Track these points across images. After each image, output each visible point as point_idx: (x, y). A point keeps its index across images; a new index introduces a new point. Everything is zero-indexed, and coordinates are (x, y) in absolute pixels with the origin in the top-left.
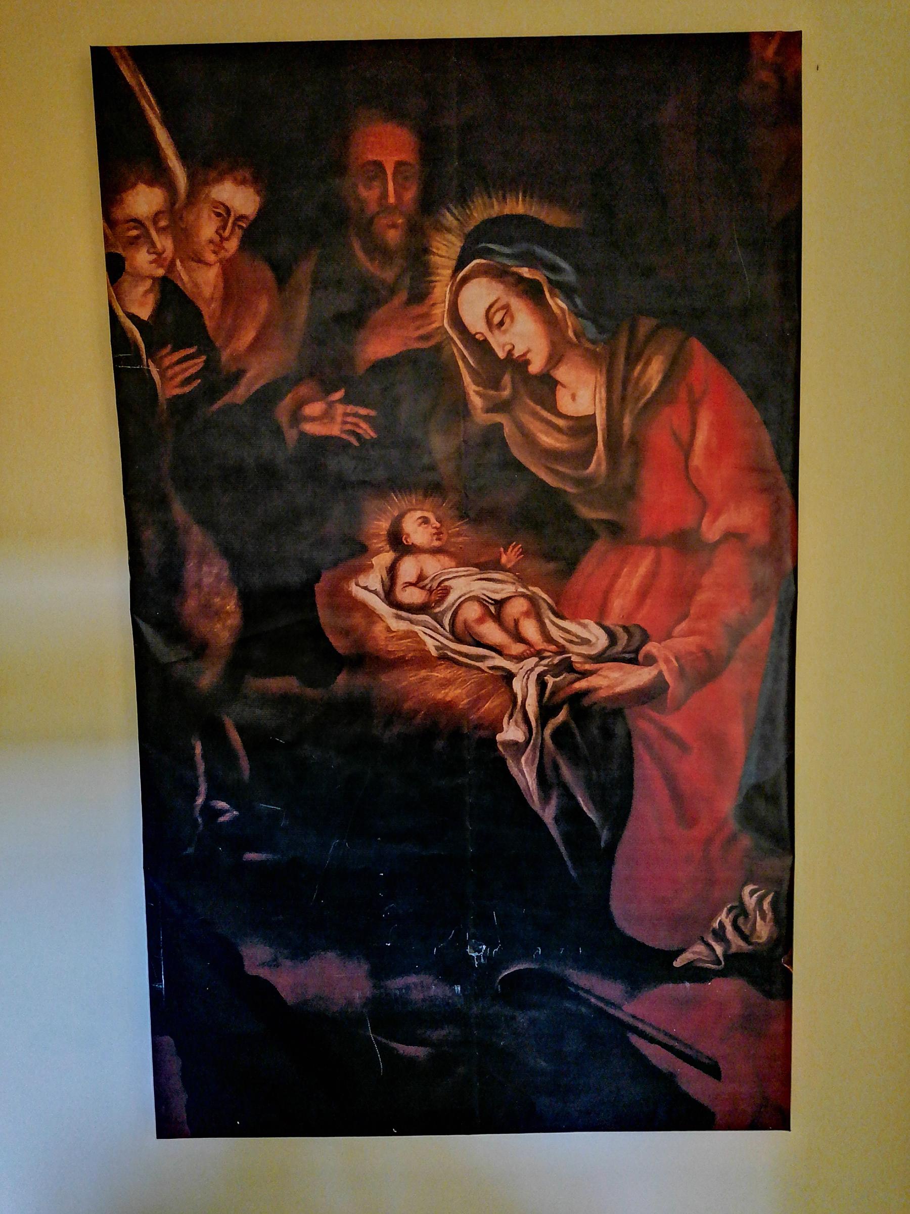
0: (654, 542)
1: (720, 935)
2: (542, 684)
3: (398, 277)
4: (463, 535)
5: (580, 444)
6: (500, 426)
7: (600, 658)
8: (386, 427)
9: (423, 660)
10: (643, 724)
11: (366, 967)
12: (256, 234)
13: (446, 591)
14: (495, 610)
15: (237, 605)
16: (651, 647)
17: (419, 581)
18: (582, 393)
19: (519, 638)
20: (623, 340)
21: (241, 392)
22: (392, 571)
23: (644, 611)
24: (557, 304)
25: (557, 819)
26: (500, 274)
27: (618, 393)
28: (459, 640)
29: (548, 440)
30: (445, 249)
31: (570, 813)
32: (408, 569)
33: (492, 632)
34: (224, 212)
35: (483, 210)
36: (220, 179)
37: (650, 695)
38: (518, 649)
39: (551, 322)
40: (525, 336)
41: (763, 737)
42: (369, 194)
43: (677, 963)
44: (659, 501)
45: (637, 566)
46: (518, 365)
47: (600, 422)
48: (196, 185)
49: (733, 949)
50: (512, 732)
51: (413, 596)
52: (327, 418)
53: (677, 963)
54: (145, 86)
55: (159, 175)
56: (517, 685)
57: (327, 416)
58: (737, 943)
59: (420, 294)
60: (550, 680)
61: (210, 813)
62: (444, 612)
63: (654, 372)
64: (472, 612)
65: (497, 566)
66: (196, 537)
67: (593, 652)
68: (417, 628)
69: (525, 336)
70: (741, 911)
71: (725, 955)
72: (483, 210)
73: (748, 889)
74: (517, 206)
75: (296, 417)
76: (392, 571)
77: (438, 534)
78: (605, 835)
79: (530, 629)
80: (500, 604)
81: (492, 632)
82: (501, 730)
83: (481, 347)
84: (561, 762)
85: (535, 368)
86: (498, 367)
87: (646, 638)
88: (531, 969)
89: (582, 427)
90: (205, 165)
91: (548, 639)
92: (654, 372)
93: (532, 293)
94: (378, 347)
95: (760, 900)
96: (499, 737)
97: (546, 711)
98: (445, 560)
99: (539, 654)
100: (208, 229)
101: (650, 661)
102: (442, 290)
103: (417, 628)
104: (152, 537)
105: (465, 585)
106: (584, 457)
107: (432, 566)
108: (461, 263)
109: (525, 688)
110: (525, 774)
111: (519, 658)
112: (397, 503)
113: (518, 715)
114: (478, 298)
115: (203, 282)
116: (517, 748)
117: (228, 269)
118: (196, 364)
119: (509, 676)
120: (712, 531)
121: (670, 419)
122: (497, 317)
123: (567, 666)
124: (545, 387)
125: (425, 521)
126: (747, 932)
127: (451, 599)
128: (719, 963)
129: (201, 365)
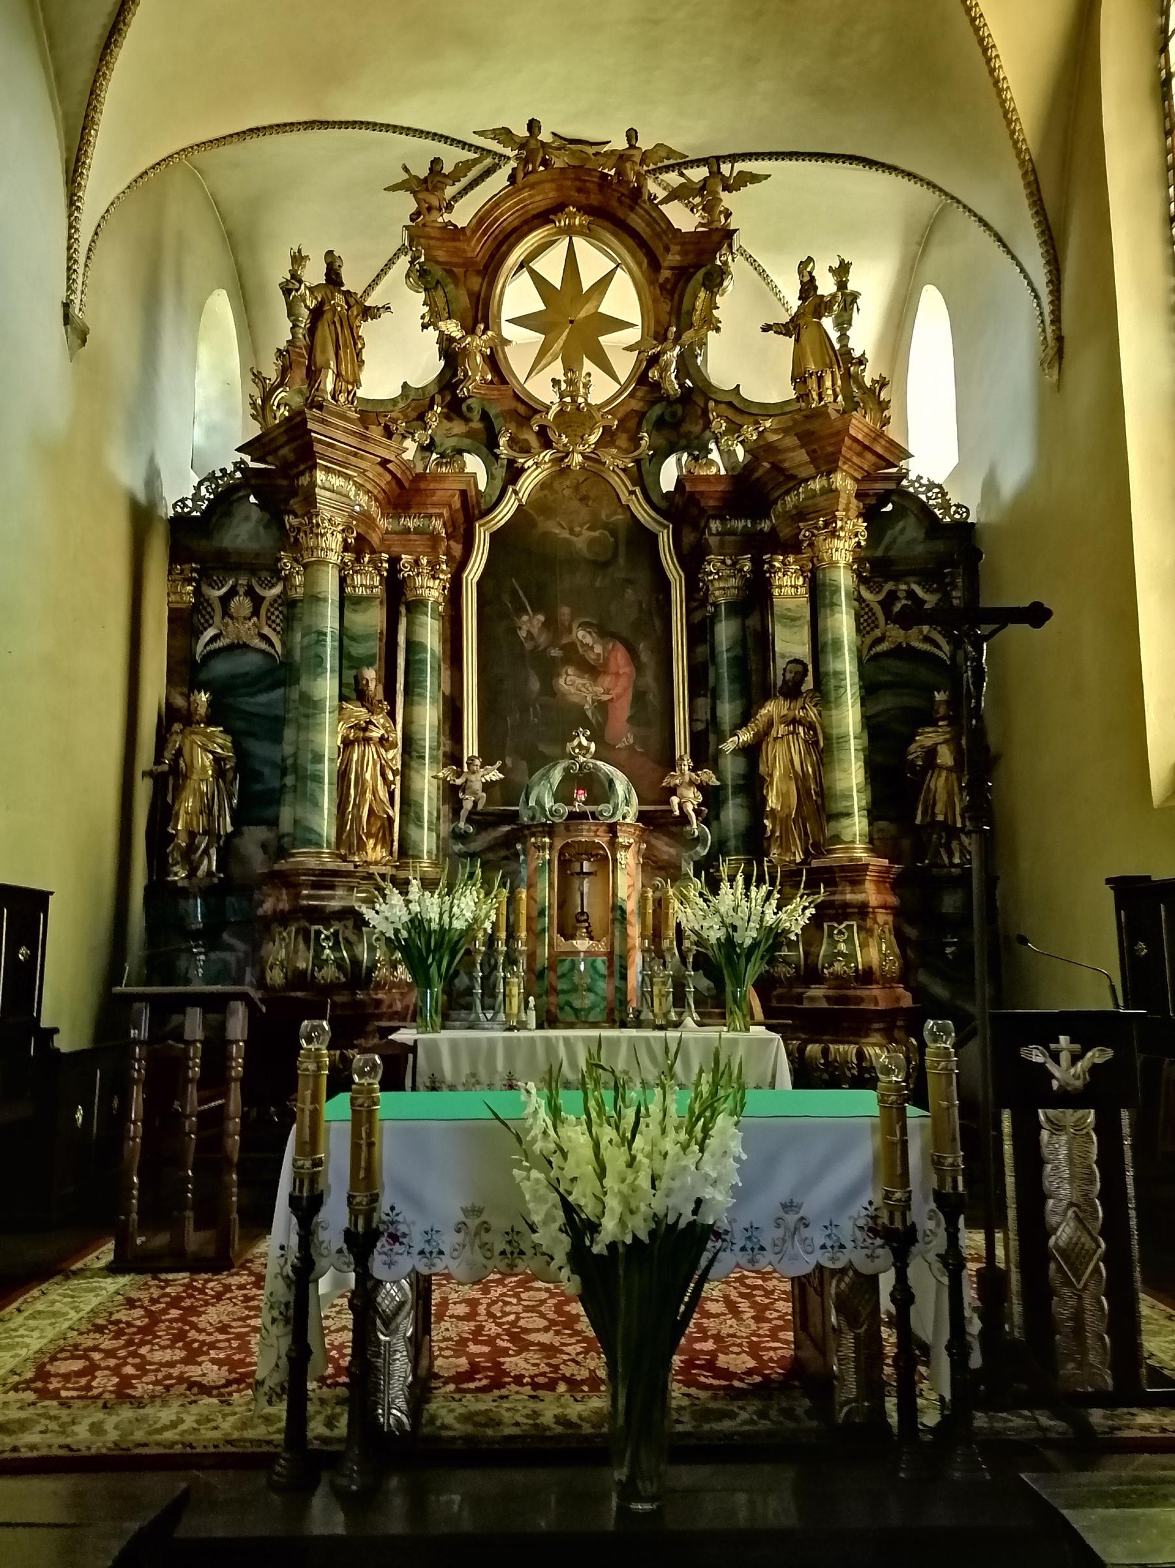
12: (544, 624)
14: (584, 685)
18: (598, 649)
27: (604, 649)
30: (575, 626)
31: (597, 721)
32: (569, 678)
40: (588, 640)
44: (613, 668)
50: (587, 707)
52: (555, 653)
55: (528, 614)
59: (571, 632)
69: (588, 640)
86: (583, 645)
89: (599, 654)
90: (536, 611)
93: (590, 633)
94: (564, 641)
97: (593, 702)
100: (535, 622)
105: (579, 681)
109: (589, 699)
110: (589, 714)
114: (581, 634)
115: (535, 631)
120: (621, 672)
121: (614, 653)
122: (584, 637)
124: (592, 648)
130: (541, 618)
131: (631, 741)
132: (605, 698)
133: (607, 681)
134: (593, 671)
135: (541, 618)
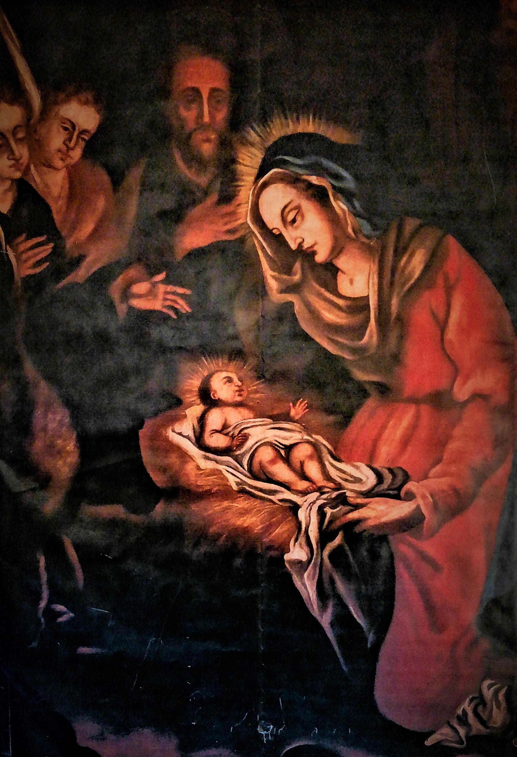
0: (414, 400)
1: (463, 720)
2: (321, 513)
3: (211, 182)
4: (259, 392)
5: (356, 320)
6: (291, 305)
7: (369, 494)
8: (199, 303)
9: (226, 493)
10: (403, 547)
11: (175, 741)
12: (96, 146)
13: (246, 438)
14: (285, 453)
15: (75, 446)
16: (410, 486)
17: (224, 429)
18: (358, 279)
19: (304, 477)
20: (392, 236)
21: (81, 274)
22: (202, 420)
23: (406, 457)
24: (340, 206)
25: (332, 624)
26: (294, 181)
28: (255, 477)
29: (330, 316)
30: (249, 160)
31: (343, 619)
32: (215, 419)
33: (281, 471)
34: (70, 127)
35: (280, 128)
36: (67, 100)
37: (409, 525)
38: (303, 485)
39: (334, 221)
40: (312, 231)
41: (501, 560)
42: (188, 115)
43: (428, 743)
44: (420, 369)
45: (400, 420)
46: (307, 255)
47: (373, 302)
48: (48, 105)
49: (474, 732)
50: (297, 553)
51: (219, 441)
52: (152, 295)
53: (428, 743)
54: (8, 24)
56: (302, 514)
57: (151, 293)
58: (477, 727)
59: (227, 197)
60: (329, 511)
61: (51, 615)
62: (244, 454)
63: (416, 263)
64: (266, 455)
65: (287, 417)
66: (44, 391)
67: (364, 488)
68: (221, 467)
69: (312, 231)
70: (480, 701)
71: (467, 737)
72: (280, 128)
73: (486, 683)
74: (308, 126)
75: (126, 294)
76: (202, 420)
77: (240, 391)
78: (371, 637)
79: (313, 469)
80: (289, 448)
81: (281, 471)
82: (288, 551)
83: (277, 240)
84: (337, 578)
85: (321, 257)
86: (291, 256)
87: (407, 478)
88: (309, 746)
89: (359, 306)
90: (56, 89)
91: (328, 477)
92: (416, 263)
93: (319, 196)
94: (194, 238)
95: (496, 693)
96: (287, 557)
98: (245, 412)
99: (320, 490)
100: (57, 140)
101: (410, 497)
102: (246, 193)
103: (221, 467)
104: (8, 390)
105: (261, 433)
106: (359, 331)
107: (235, 417)
108: (262, 171)
109: (308, 517)
110: (307, 587)
111: (304, 493)
112: (207, 365)
113: (302, 539)
114: (276, 199)
115: (53, 184)
116: (301, 566)
117: (73, 175)
118: (45, 250)
119: (295, 508)
120: (462, 392)
121: (429, 301)
122: (291, 217)
123: (342, 500)
125: (230, 380)
126: (485, 718)
127: (249, 443)
128: (462, 743)
129: (50, 251)
130: (85, 116)
131: (498, 717)
132: (382, 512)
133: (390, 430)
134: (329, 391)
135: (85, 116)
